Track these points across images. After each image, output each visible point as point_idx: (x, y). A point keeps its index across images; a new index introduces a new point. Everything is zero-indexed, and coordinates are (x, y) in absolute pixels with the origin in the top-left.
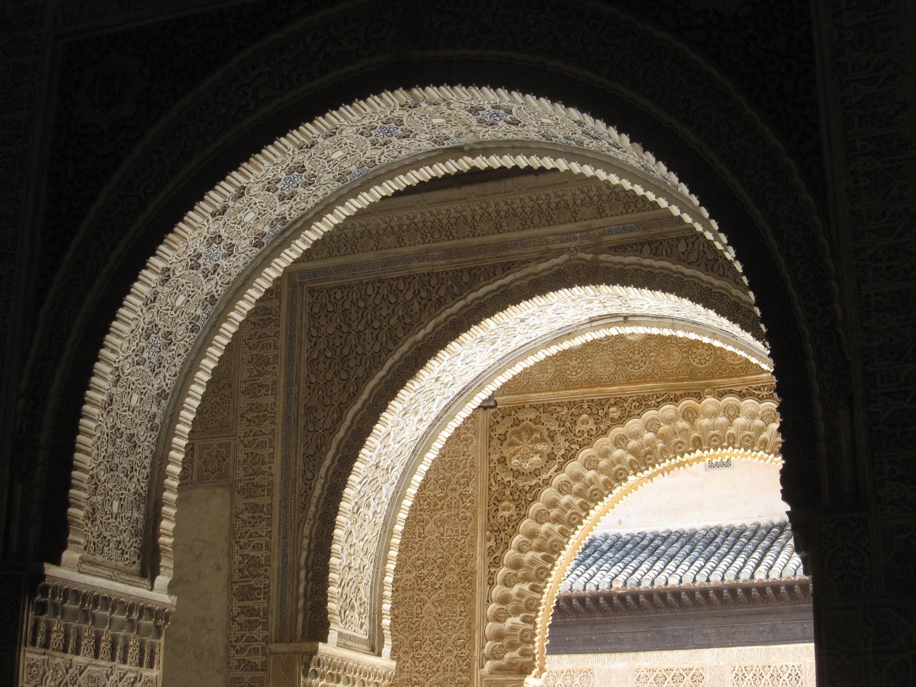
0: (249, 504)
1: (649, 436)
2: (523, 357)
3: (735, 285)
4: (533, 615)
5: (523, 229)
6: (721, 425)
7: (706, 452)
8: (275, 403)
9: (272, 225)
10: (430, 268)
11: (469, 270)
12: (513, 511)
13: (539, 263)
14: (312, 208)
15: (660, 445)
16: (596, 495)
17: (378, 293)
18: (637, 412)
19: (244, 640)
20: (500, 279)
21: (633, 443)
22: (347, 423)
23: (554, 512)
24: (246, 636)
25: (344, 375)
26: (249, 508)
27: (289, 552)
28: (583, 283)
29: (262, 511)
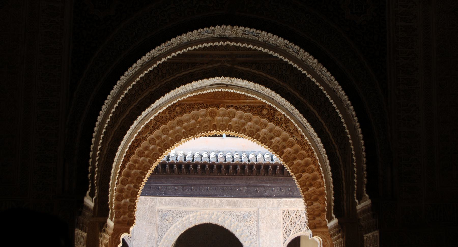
1: (192, 121)
7: (218, 131)
16: (166, 146)
18: (188, 110)
20: (191, 69)
21: (185, 124)
22: (119, 124)
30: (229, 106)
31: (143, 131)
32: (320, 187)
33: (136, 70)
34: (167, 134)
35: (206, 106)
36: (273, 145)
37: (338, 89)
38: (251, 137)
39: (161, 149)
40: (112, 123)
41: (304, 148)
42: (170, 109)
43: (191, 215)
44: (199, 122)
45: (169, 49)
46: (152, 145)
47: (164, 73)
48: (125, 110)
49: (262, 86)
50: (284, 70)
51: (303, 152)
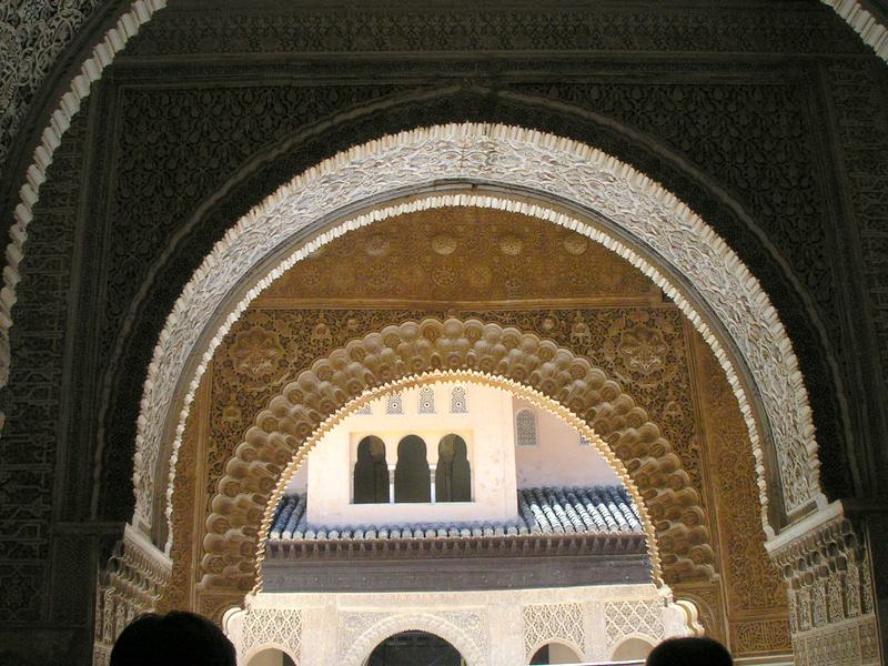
0: (30, 338)
4: (256, 527)
5: (412, 49)
6: (460, 348)
7: (445, 372)
8: (74, 216)
11: (338, 89)
12: (238, 417)
16: (327, 407)
17: (217, 102)
18: (376, 326)
19: (14, 515)
21: (370, 357)
23: (282, 421)
24: (18, 511)
25: (168, 192)
26: (31, 343)
29: (49, 348)
32: (682, 488)
34: (330, 380)
43: (390, 618)
51: (640, 410)
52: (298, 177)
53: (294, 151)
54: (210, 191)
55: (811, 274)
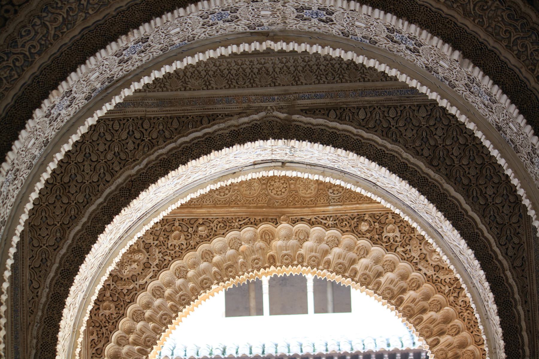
2: (194, 190)
3: (405, 149)
5: (230, 87)
6: (293, 247)
7: (279, 268)
9: (103, 83)
10: (143, 113)
11: (178, 118)
12: (113, 311)
13: (241, 117)
14: (134, 70)
15: (241, 260)
16: (184, 300)
17: (94, 131)
18: (222, 232)
20: (206, 128)
21: (217, 258)
22: (69, 241)
23: (148, 313)
25: (65, 200)
27: (20, 349)
28: (277, 137)
30: (296, 220)
31: (140, 273)
33: (76, 106)
34: (185, 277)
35: (254, 223)
36: (382, 288)
37: (509, 119)
38: (340, 276)
39: (175, 306)
40: (56, 240)
41: (439, 289)
42: (188, 231)
44: (243, 252)
45: (144, 60)
46: (158, 298)
47: (153, 137)
48: (79, 213)
49: (351, 154)
50: (393, 118)
51: (439, 296)
52: (153, 185)
53: (149, 166)
54: (94, 198)
55: (510, 246)
